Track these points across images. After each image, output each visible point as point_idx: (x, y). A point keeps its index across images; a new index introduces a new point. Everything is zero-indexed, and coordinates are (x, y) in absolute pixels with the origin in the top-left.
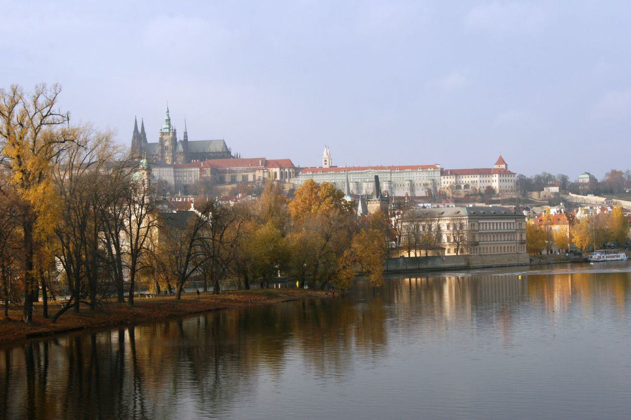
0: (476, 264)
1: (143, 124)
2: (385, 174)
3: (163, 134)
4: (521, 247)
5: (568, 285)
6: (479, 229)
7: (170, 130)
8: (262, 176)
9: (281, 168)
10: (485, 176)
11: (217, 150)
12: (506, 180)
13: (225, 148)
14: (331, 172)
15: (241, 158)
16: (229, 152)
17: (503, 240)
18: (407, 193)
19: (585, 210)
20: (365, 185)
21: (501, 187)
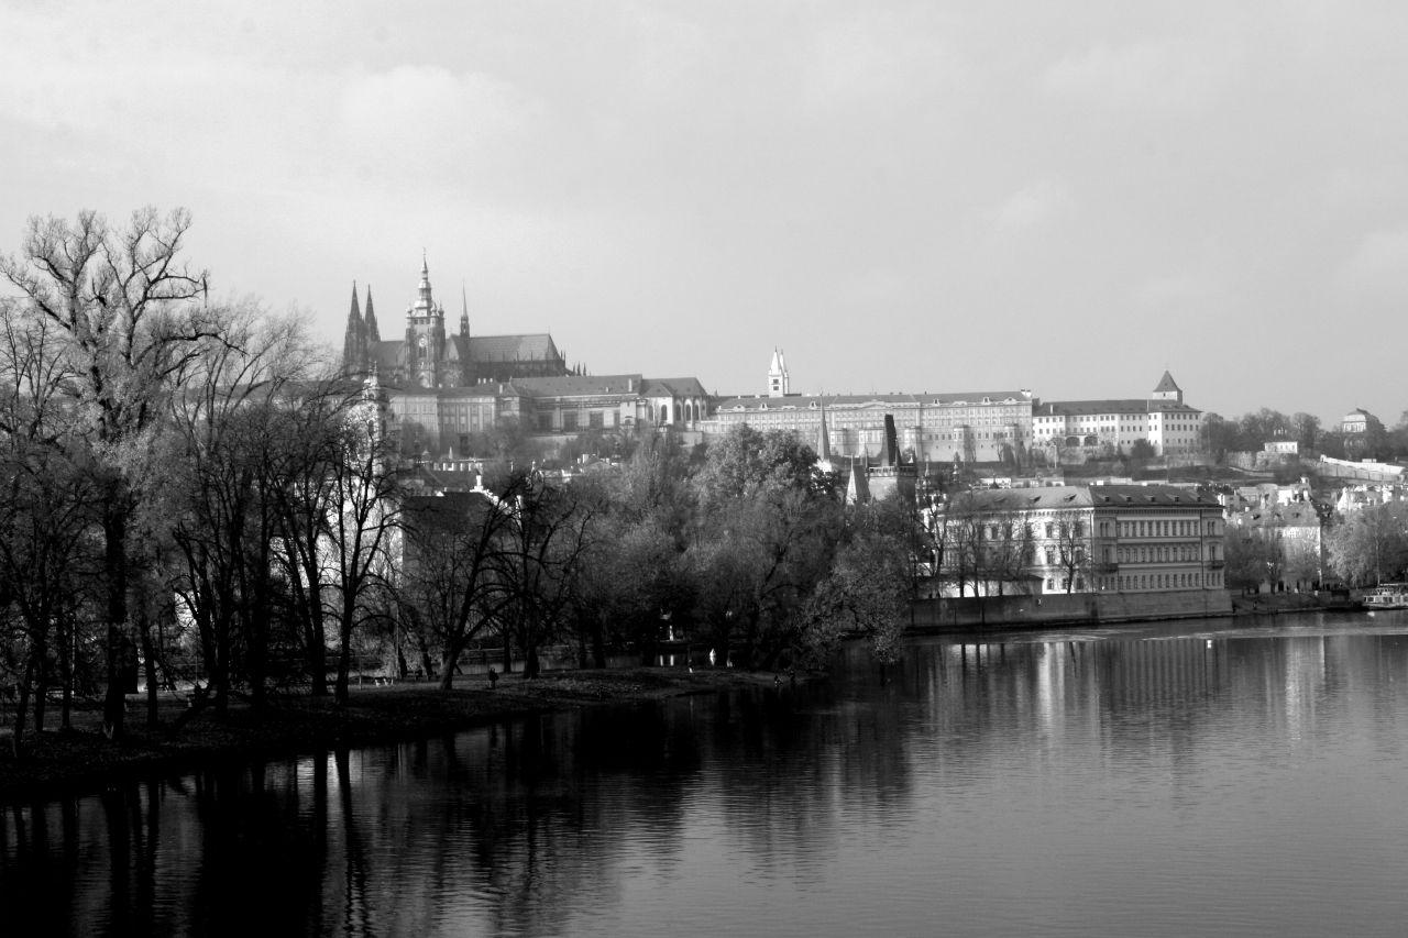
0: (1111, 613)
1: (370, 299)
2: (908, 412)
3: (414, 320)
4: (1213, 575)
5: (1319, 658)
6: (1119, 536)
7: (429, 313)
8: (634, 415)
9: (675, 398)
10: (1131, 417)
11: (535, 358)
12: (1173, 426)
13: (551, 353)
14: (789, 407)
15: (588, 374)
16: (560, 362)
17: (1172, 559)
18: (957, 454)
19: (1357, 493)
20: (862, 436)
21: (1167, 441)
